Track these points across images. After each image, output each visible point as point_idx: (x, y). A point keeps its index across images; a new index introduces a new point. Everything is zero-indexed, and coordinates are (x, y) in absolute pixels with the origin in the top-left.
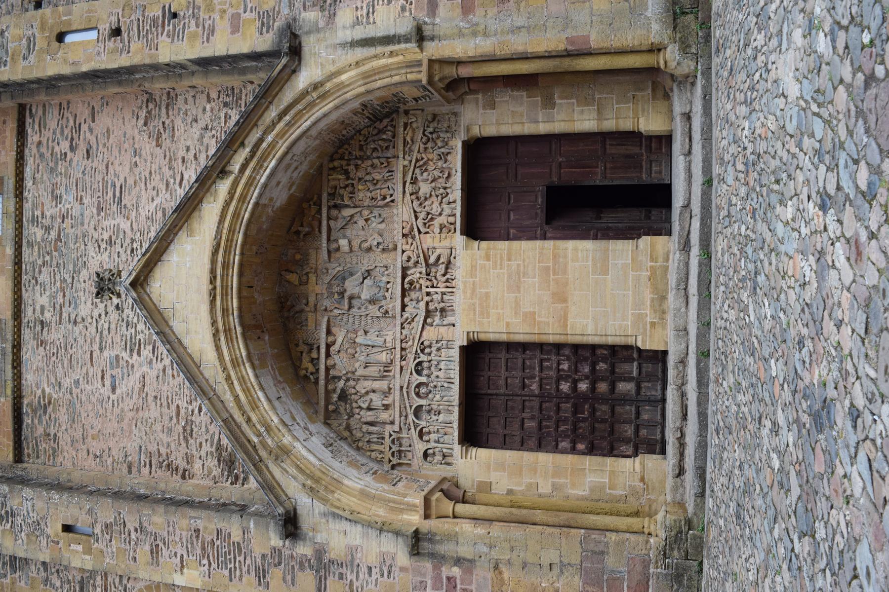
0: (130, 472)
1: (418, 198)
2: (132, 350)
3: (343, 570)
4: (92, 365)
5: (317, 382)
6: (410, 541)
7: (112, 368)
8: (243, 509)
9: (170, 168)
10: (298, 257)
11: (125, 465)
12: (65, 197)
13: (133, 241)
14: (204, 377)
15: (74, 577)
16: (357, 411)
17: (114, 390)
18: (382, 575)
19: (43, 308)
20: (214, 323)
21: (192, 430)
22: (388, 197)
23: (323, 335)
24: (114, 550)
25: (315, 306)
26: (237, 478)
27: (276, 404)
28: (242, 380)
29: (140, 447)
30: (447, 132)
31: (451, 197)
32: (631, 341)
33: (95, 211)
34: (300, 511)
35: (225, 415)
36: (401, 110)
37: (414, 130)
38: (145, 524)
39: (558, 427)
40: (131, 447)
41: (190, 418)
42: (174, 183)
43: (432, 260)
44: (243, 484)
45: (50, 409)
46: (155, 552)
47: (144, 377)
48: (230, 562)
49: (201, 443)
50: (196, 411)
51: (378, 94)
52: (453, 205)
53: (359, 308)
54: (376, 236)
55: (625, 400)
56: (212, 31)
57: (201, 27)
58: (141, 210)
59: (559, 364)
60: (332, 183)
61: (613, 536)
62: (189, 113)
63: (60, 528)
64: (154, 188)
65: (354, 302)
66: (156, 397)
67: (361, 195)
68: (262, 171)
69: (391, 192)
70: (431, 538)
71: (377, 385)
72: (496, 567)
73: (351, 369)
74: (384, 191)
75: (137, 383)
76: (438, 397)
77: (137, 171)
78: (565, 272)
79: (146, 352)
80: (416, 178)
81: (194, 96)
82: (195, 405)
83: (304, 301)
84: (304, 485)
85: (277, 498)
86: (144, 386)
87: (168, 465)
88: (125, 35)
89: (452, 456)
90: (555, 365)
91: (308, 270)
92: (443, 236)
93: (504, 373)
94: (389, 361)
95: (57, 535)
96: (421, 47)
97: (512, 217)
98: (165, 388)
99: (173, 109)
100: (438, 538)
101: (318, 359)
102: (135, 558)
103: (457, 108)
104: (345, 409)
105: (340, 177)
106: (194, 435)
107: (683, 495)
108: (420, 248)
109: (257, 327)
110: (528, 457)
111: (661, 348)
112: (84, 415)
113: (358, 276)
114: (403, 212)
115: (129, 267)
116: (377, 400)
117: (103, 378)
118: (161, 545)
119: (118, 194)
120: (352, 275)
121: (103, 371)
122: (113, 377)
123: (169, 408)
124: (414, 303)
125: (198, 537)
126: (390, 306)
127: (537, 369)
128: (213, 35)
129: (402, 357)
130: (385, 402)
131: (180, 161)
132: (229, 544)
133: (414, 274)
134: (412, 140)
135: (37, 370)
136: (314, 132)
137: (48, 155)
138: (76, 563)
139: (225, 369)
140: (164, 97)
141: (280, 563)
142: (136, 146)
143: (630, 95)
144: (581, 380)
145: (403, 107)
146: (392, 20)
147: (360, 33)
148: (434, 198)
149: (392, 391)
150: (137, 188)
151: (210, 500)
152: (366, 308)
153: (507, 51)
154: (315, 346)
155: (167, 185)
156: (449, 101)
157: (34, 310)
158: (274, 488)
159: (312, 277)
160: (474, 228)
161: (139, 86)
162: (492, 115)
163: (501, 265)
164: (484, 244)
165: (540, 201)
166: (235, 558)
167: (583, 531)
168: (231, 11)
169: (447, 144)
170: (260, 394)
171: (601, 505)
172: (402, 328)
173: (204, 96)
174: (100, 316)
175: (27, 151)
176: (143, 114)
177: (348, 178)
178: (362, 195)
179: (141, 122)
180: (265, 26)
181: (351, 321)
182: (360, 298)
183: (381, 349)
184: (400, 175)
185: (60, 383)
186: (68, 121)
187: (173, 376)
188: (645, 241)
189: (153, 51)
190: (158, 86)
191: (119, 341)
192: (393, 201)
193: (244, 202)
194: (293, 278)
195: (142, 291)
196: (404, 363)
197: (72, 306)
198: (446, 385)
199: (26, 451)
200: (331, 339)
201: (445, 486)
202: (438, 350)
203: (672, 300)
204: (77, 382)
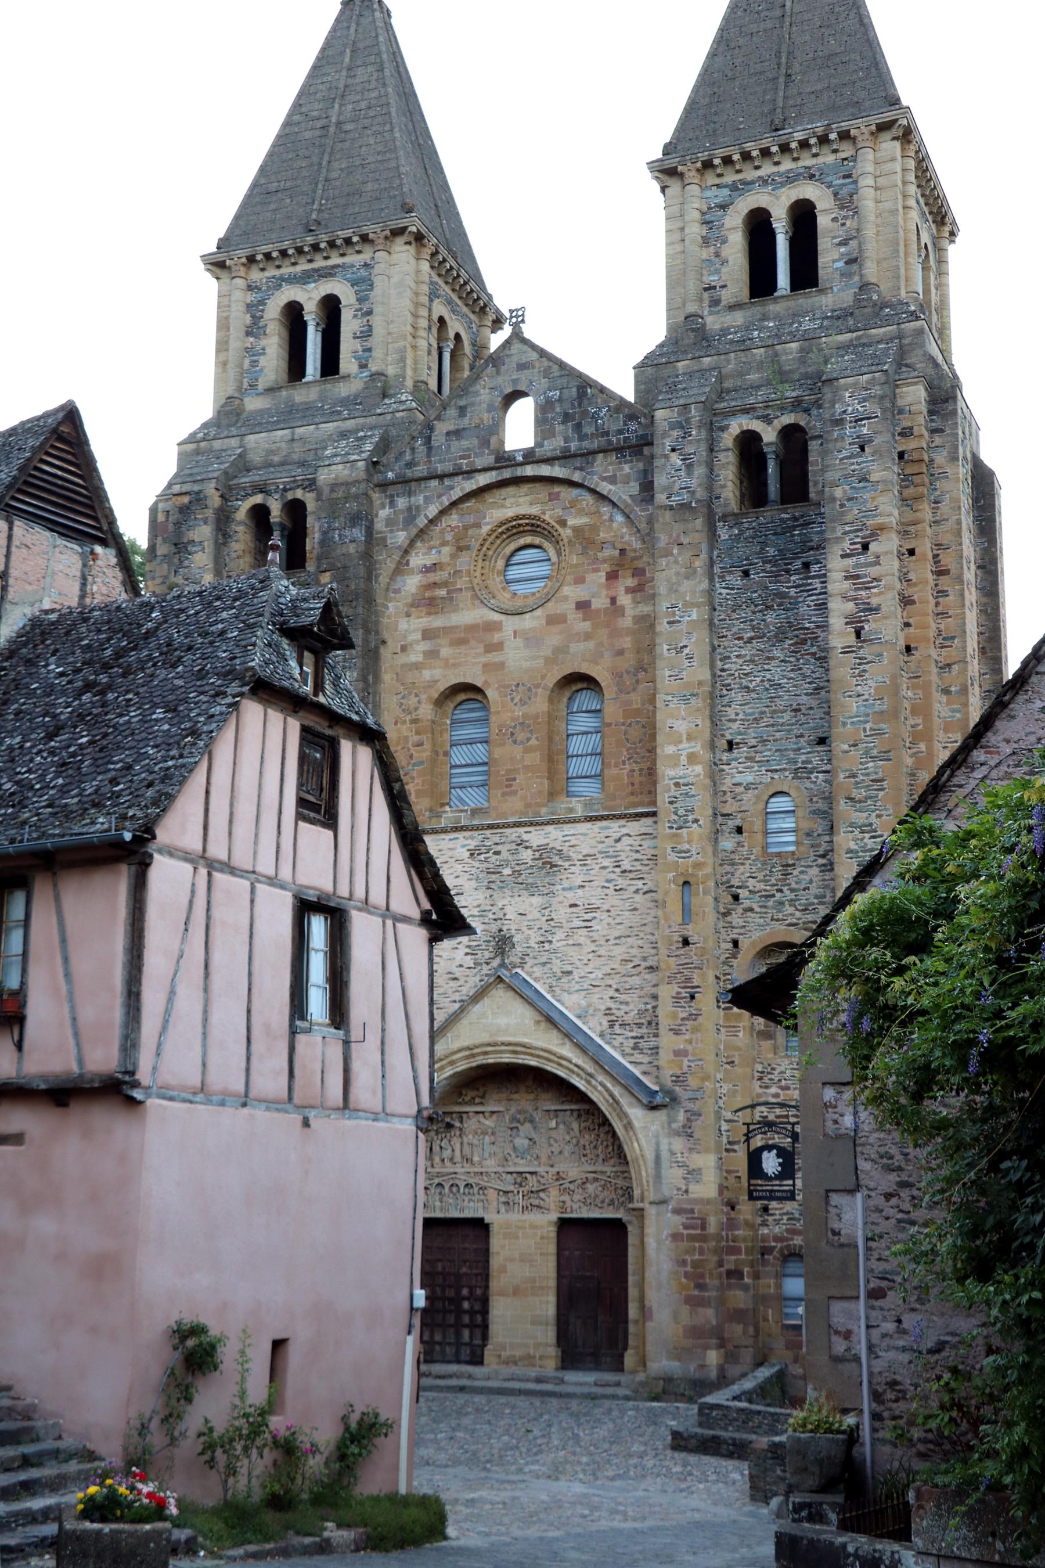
2: (469, 947)
5: (460, 1104)
13: (550, 942)
20: (476, 1047)
32: (490, 1341)
43: (542, 1195)
55: (458, 1335)
56: (677, 1032)
71: (458, 1153)
78: (533, 1295)
97: (577, 1253)
111: (486, 1362)
113: (533, 1135)
114: (574, 1171)
116: (447, 1154)
120: (535, 1128)
139: (446, 1057)
147: (665, 1155)
164: (553, 1235)
168: (690, 1048)
175: (622, 822)
177: (599, 1125)
178: (587, 1137)
180: (678, 1079)
184: (599, 1169)
188: (553, 1351)
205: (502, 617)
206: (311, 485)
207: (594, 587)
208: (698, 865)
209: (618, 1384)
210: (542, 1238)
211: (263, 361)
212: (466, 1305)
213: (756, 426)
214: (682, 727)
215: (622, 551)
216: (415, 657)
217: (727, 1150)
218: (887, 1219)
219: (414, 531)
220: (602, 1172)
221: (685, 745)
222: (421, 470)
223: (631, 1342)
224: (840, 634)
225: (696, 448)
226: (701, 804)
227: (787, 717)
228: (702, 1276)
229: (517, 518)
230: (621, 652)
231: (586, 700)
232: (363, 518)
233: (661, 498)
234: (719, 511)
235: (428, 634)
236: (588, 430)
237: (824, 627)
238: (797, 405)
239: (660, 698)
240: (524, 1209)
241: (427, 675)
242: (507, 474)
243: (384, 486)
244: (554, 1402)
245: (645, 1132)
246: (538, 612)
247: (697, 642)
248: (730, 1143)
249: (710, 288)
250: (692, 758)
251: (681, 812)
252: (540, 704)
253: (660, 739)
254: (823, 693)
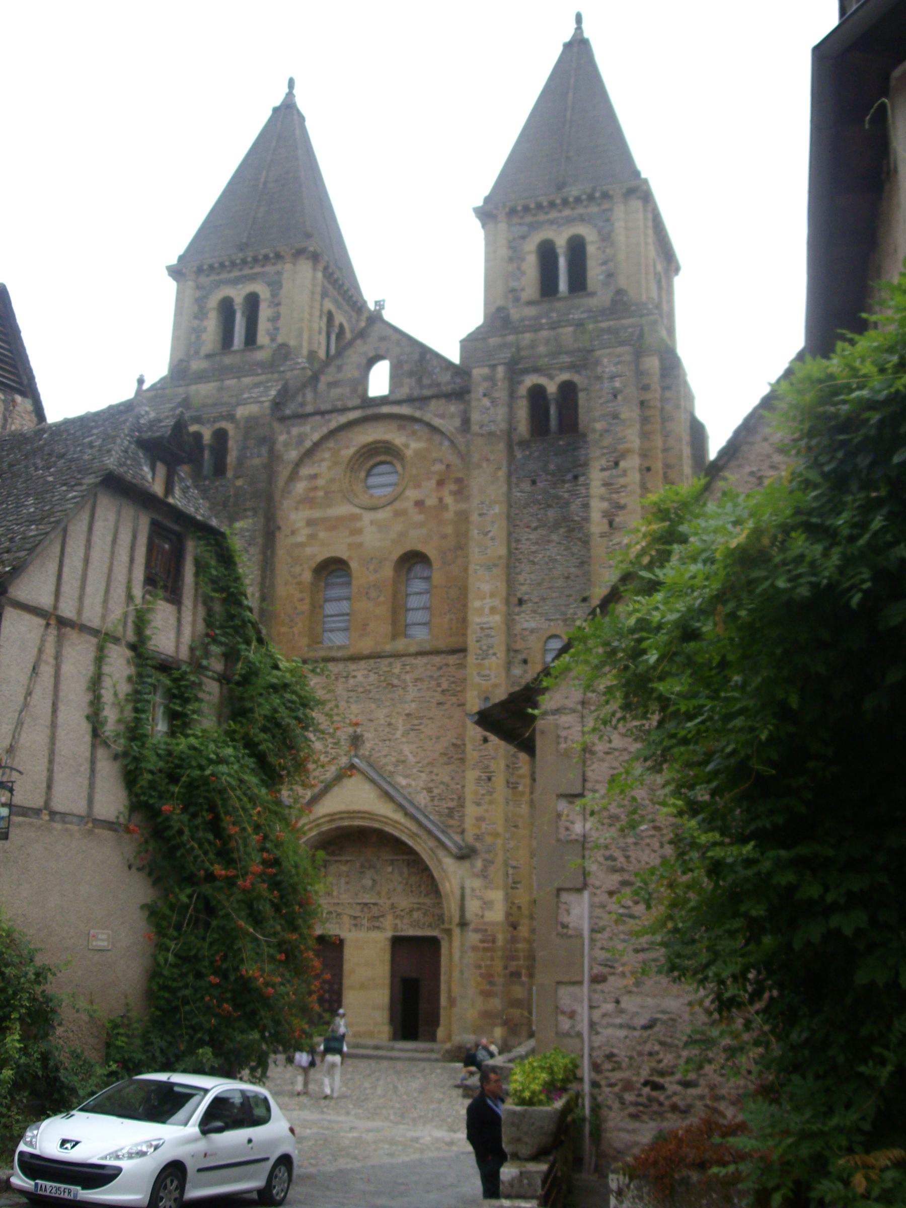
19: (355, 677)
43: (381, 919)
114: (404, 902)
147: (468, 892)
160: (398, 942)
164: (388, 948)
179: (455, 741)
180: (478, 838)
184: (421, 900)
205: (362, 511)
206: (231, 417)
207: (428, 492)
208: (495, 686)
209: (432, 1051)
211: (204, 336)
213: (542, 380)
214: (486, 587)
215: (448, 466)
216: (300, 538)
217: (512, 888)
218: (610, 913)
219: (302, 450)
221: (488, 600)
222: (309, 409)
223: (442, 1021)
224: (597, 524)
225: (501, 394)
226: (499, 643)
227: (560, 583)
228: (492, 976)
229: (375, 442)
230: (444, 537)
231: (419, 570)
232: (268, 441)
233: (475, 428)
234: (516, 438)
235: (310, 523)
236: (426, 381)
237: (587, 519)
238: (572, 367)
239: (472, 567)
240: (369, 929)
241: (308, 551)
242: (370, 412)
243: (283, 419)
244: (385, 1063)
245: (453, 875)
246: (388, 508)
247: (499, 529)
248: (514, 883)
249: (513, 290)
250: (493, 610)
251: (485, 648)
252: (388, 571)
253: (471, 596)
254: (586, 567)
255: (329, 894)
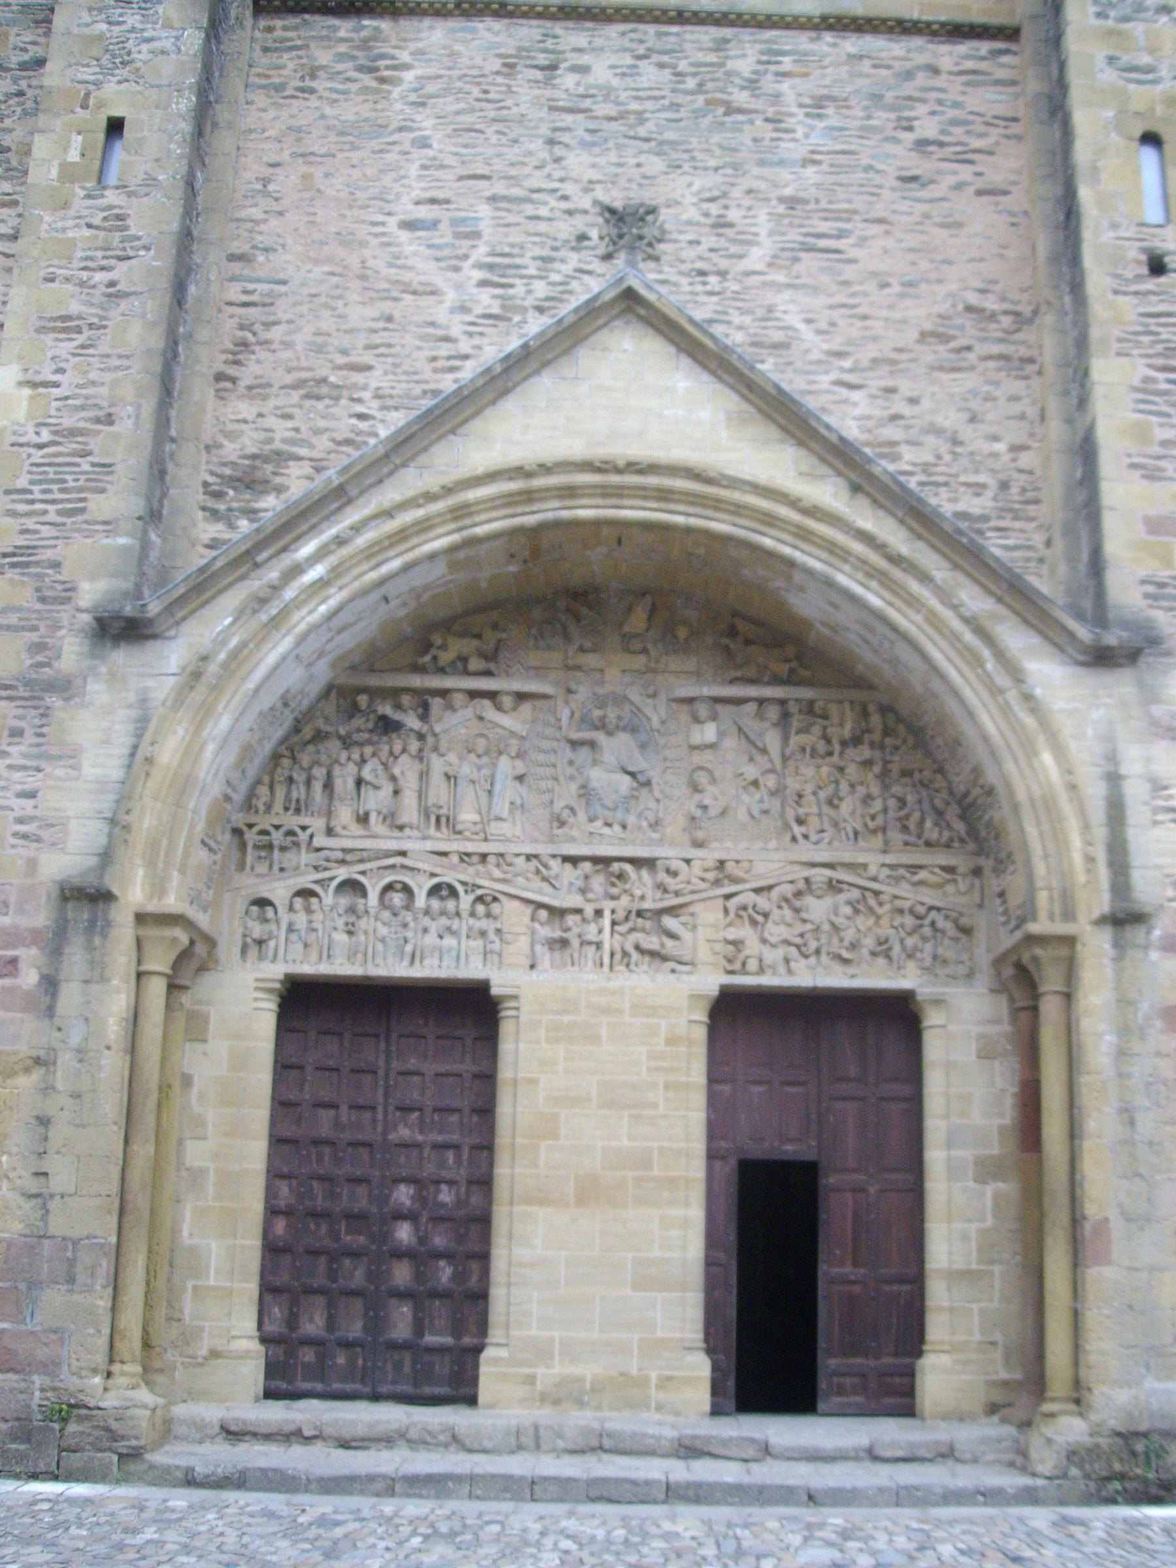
0: (232, 258)
1: (798, 894)
3: (30, 738)
4: (461, 178)
6: (91, 881)
7: (454, 222)
8: (153, 515)
9: (875, 361)
10: (682, 632)
11: (246, 248)
12: (820, 125)
13: (722, 274)
14: (432, 444)
15: (10, 131)
16: (356, 757)
17: (409, 225)
18: (20, 821)
19: (584, 70)
20: (545, 469)
21: (319, 398)
22: (803, 829)
23: (517, 685)
24: (71, 234)
25: (578, 668)
26: (218, 495)
27: (376, 595)
28: (424, 527)
29: (284, 282)
30: (935, 957)
31: (799, 965)
32: (496, 1334)
33: (788, 192)
34: (152, 646)
35: (353, 492)
36: (982, 861)
37: (940, 886)
38: (124, 305)
39: (321, 1178)
40: (287, 262)
41: (345, 393)
42: (843, 370)
43: (669, 922)
44: (204, 509)
45: (368, 80)
46: (66, 325)
47: (433, 293)
48: (45, 491)
49: (289, 417)
50: (360, 409)
51: (1012, 826)
52: (782, 969)
53: (571, 763)
54: (722, 803)
55: (376, 1322)
56: (1152, 475)
57: (1160, 451)
58: (787, 295)
59: (451, 1183)
60: (834, 710)
61: (104, 1303)
62: (989, 405)
63: (117, 113)
64: (833, 324)
65: (584, 752)
66: (390, 319)
67: (808, 771)
68: (860, 576)
69: (814, 837)
70: (98, 928)
71: (409, 798)
72: (38, 1061)
73: (443, 745)
74: (814, 822)
75: (422, 278)
76: (383, 931)
77: (871, 287)
79: (486, 300)
80: (840, 891)
81: (1022, 417)
82: (371, 407)
83: (588, 644)
84: (204, 659)
85: (182, 600)
86: (415, 293)
87: (245, 344)
88: (1151, 284)
89: (261, 958)
90: (444, 1174)
91: (653, 653)
92: (719, 947)
93: (430, 1068)
94: (459, 827)
95: (101, 105)
96: (1101, 921)
97: (757, 1089)
98: (410, 340)
99: (999, 370)
100: (97, 941)
101: (467, 673)
102: (52, 280)
103: (983, 982)
104: (359, 730)
105: (848, 726)
106: (308, 403)
107: (185, 1439)
108: (695, 897)
109: (536, 553)
110: (258, 1116)
111: (484, 1395)
112: (355, 156)
113: (639, 763)
114: (770, 861)
115: (664, 281)
116: (376, 800)
117: (433, 201)
118: (81, 339)
119: (823, 243)
120: (643, 746)
121: (447, 202)
122: (435, 224)
123: (368, 347)
124: (580, 883)
125: (98, 421)
126: (575, 833)
127: (440, 1138)
128: (1143, 476)
129: (468, 855)
130: (373, 818)
131: (889, 383)
132: (81, 490)
133: (642, 883)
134: (921, 883)
135: (453, 54)
136: (936, 685)
137: (909, 89)
138: (41, 147)
139: (448, 490)
140: (1023, 351)
141: (43, 600)
142: (923, 287)
143: (999, 1337)
144: (417, 1229)
145: (987, 864)
146: (1159, 861)
147: (1135, 792)
148: (800, 928)
149: (397, 833)
150: (834, 288)
151: (173, 440)
152: (572, 778)
153: (1087, 1098)
154: (492, 666)
155: (839, 355)
156: (998, 962)
157: (580, 50)
158: (200, 594)
159: (640, 661)
160: (737, 1014)
161: (1048, 303)
162: (966, 1054)
163: (658, 1069)
164: (700, 1034)
165: (789, 1147)
166: (54, 502)
167: (114, 1239)
169: (910, 956)
170: (396, 564)
171: (163, 1274)
172: (529, 857)
173: (1020, 438)
174: (565, 198)
175: (918, 41)
176: (991, 304)
177: (844, 744)
178: (807, 775)
179: (973, 299)
180: (1158, 590)
181: (546, 745)
182: (595, 763)
183: (484, 809)
184: (847, 857)
185: (423, 104)
186: (984, 135)
187: (434, 359)
188: (701, 1367)
189: (1116, 346)
190: (1047, 342)
191: (511, 239)
192: (794, 839)
193: (796, 535)
194: (638, 621)
195: (615, 312)
196: (455, 859)
197: (588, 138)
198: (409, 948)
199: (278, 23)
200: (507, 701)
201: (200, 949)
202: (483, 934)
203: (579, 1419)
204: (423, 143)
210: (672, 1041)
212: (404, 1233)
220: (851, 867)
255: (445, 821)
